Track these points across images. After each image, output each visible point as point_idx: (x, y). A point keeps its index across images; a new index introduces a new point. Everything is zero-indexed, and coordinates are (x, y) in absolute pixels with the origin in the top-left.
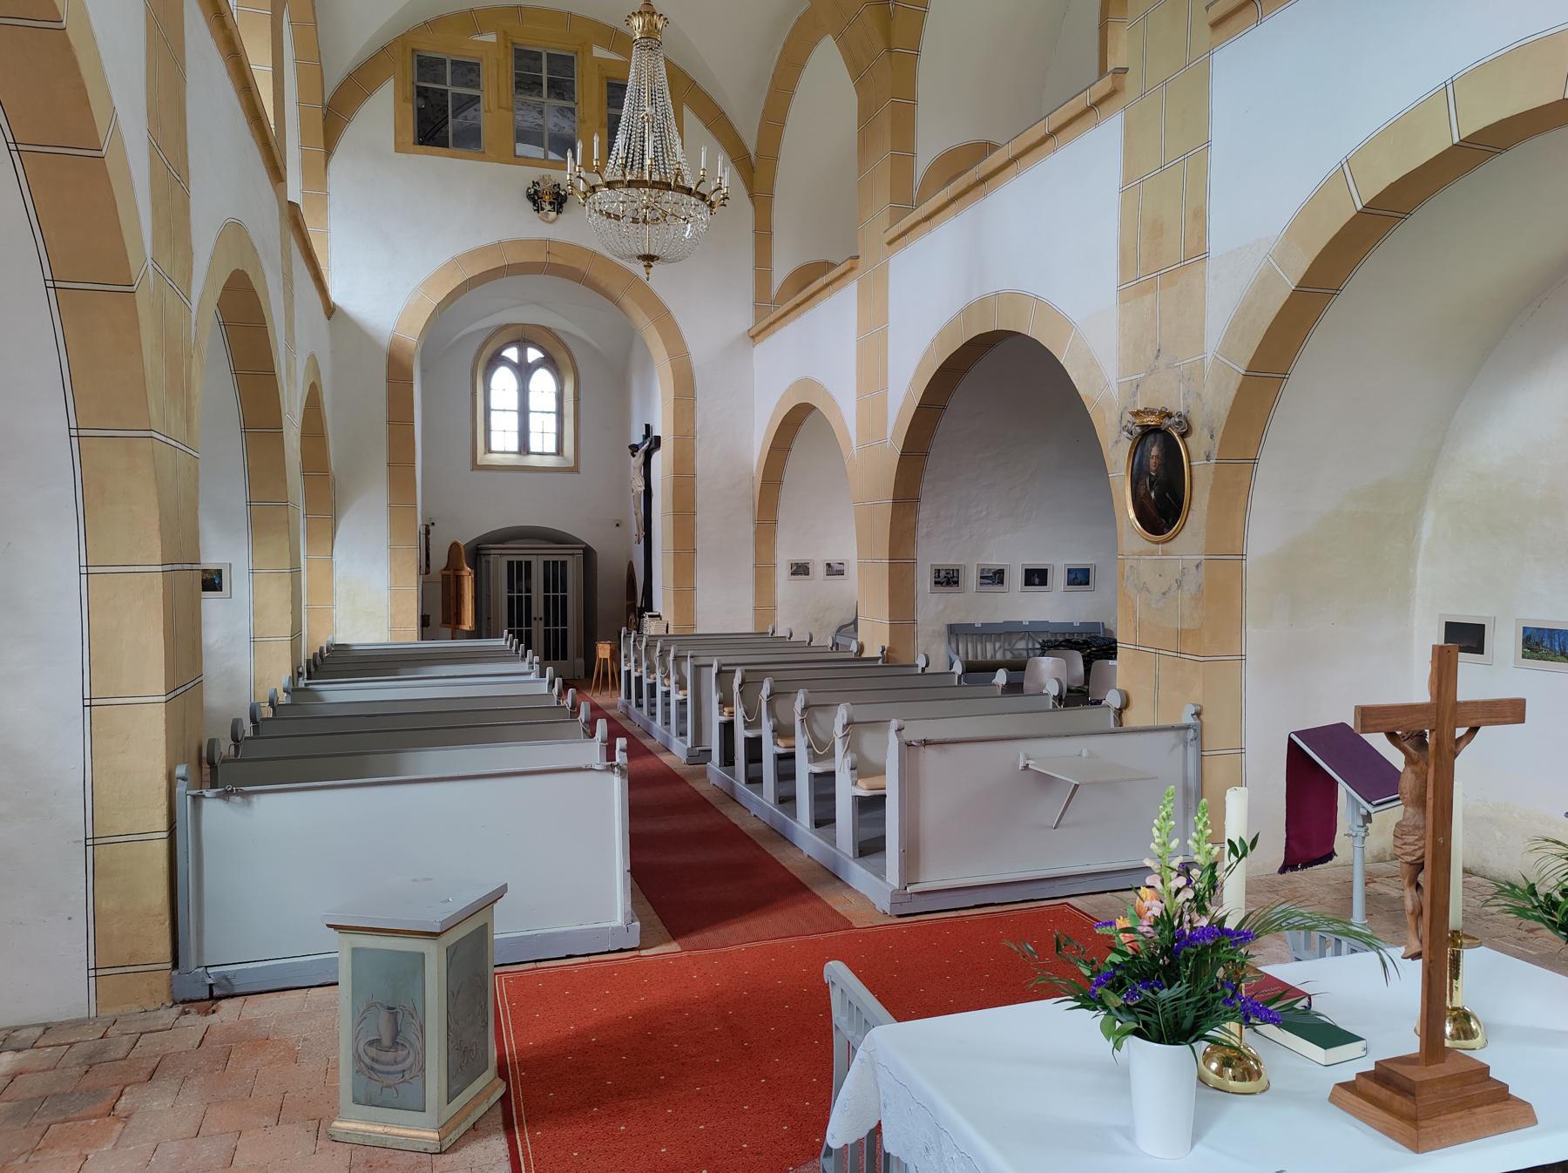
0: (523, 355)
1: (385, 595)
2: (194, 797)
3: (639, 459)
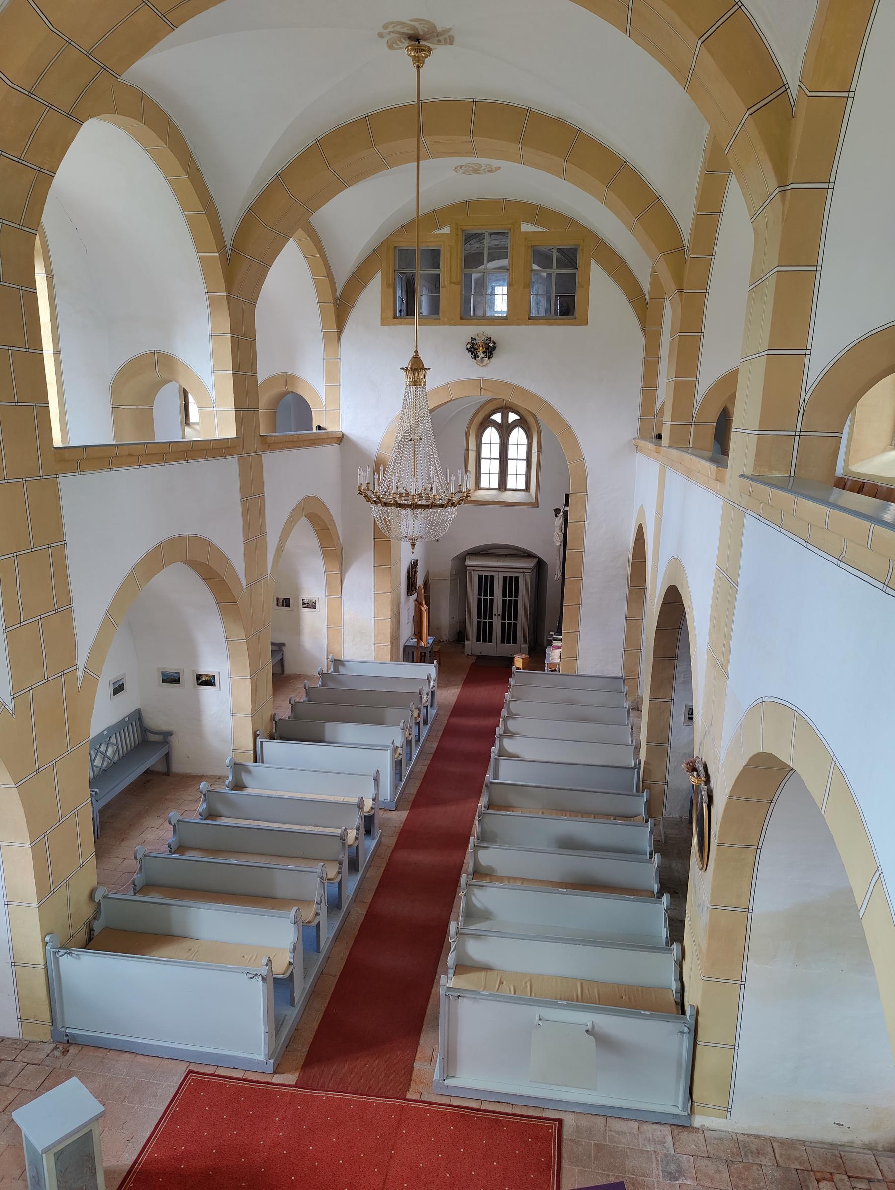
0: (505, 417)
2: (55, 953)
3: (559, 521)
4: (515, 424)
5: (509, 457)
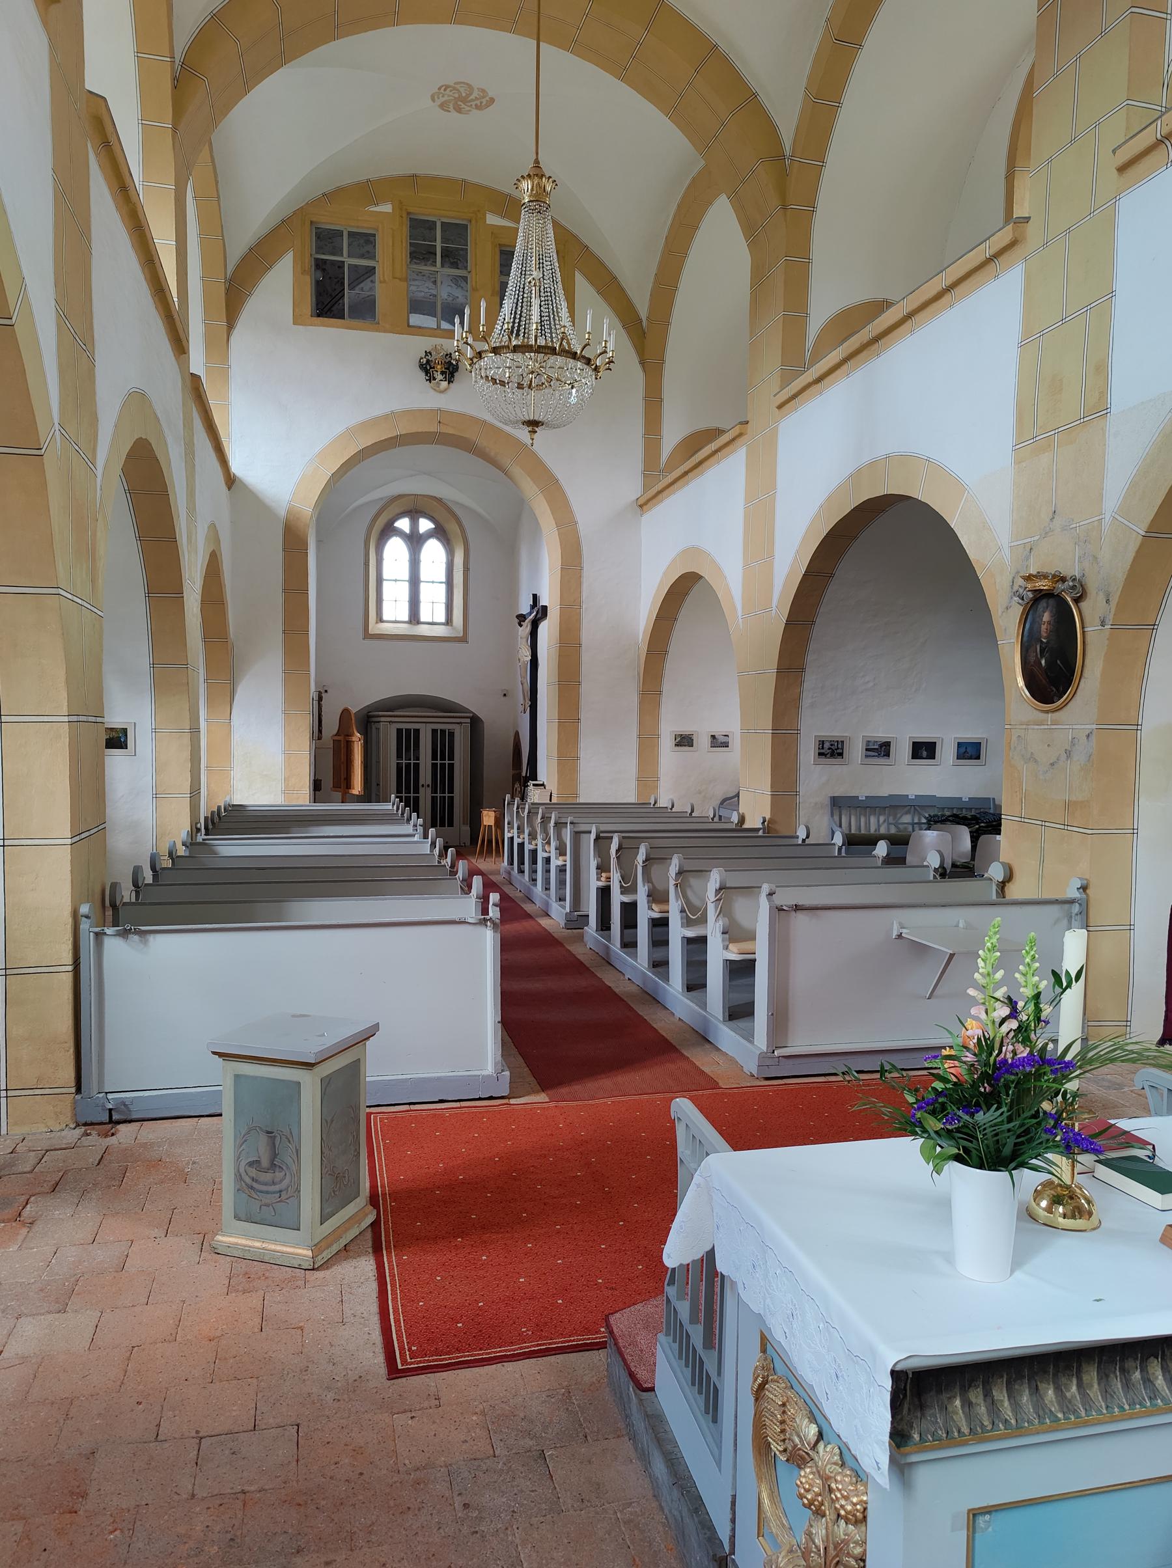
1: (280, 758)
2: (97, 934)
3: (526, 628)
4: (430, 535)
5: (422, 579)
